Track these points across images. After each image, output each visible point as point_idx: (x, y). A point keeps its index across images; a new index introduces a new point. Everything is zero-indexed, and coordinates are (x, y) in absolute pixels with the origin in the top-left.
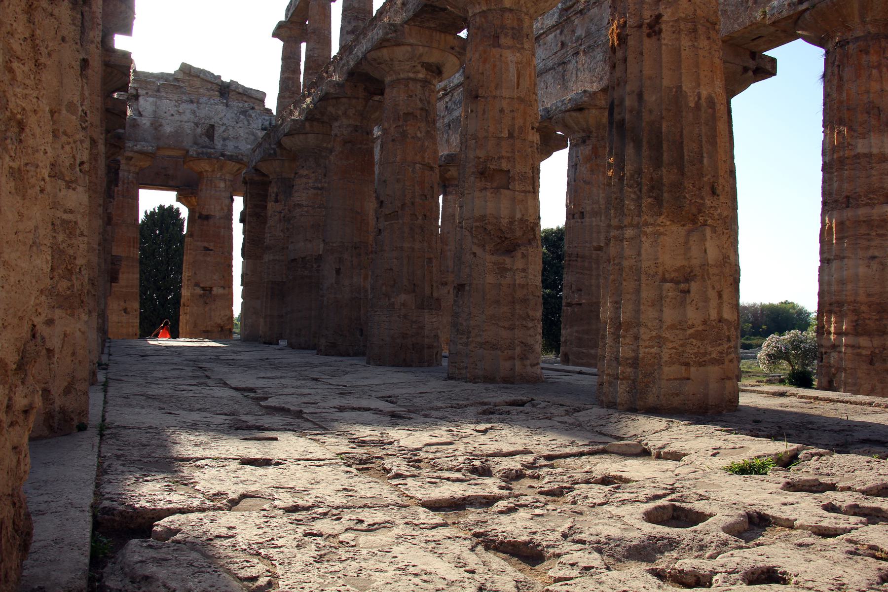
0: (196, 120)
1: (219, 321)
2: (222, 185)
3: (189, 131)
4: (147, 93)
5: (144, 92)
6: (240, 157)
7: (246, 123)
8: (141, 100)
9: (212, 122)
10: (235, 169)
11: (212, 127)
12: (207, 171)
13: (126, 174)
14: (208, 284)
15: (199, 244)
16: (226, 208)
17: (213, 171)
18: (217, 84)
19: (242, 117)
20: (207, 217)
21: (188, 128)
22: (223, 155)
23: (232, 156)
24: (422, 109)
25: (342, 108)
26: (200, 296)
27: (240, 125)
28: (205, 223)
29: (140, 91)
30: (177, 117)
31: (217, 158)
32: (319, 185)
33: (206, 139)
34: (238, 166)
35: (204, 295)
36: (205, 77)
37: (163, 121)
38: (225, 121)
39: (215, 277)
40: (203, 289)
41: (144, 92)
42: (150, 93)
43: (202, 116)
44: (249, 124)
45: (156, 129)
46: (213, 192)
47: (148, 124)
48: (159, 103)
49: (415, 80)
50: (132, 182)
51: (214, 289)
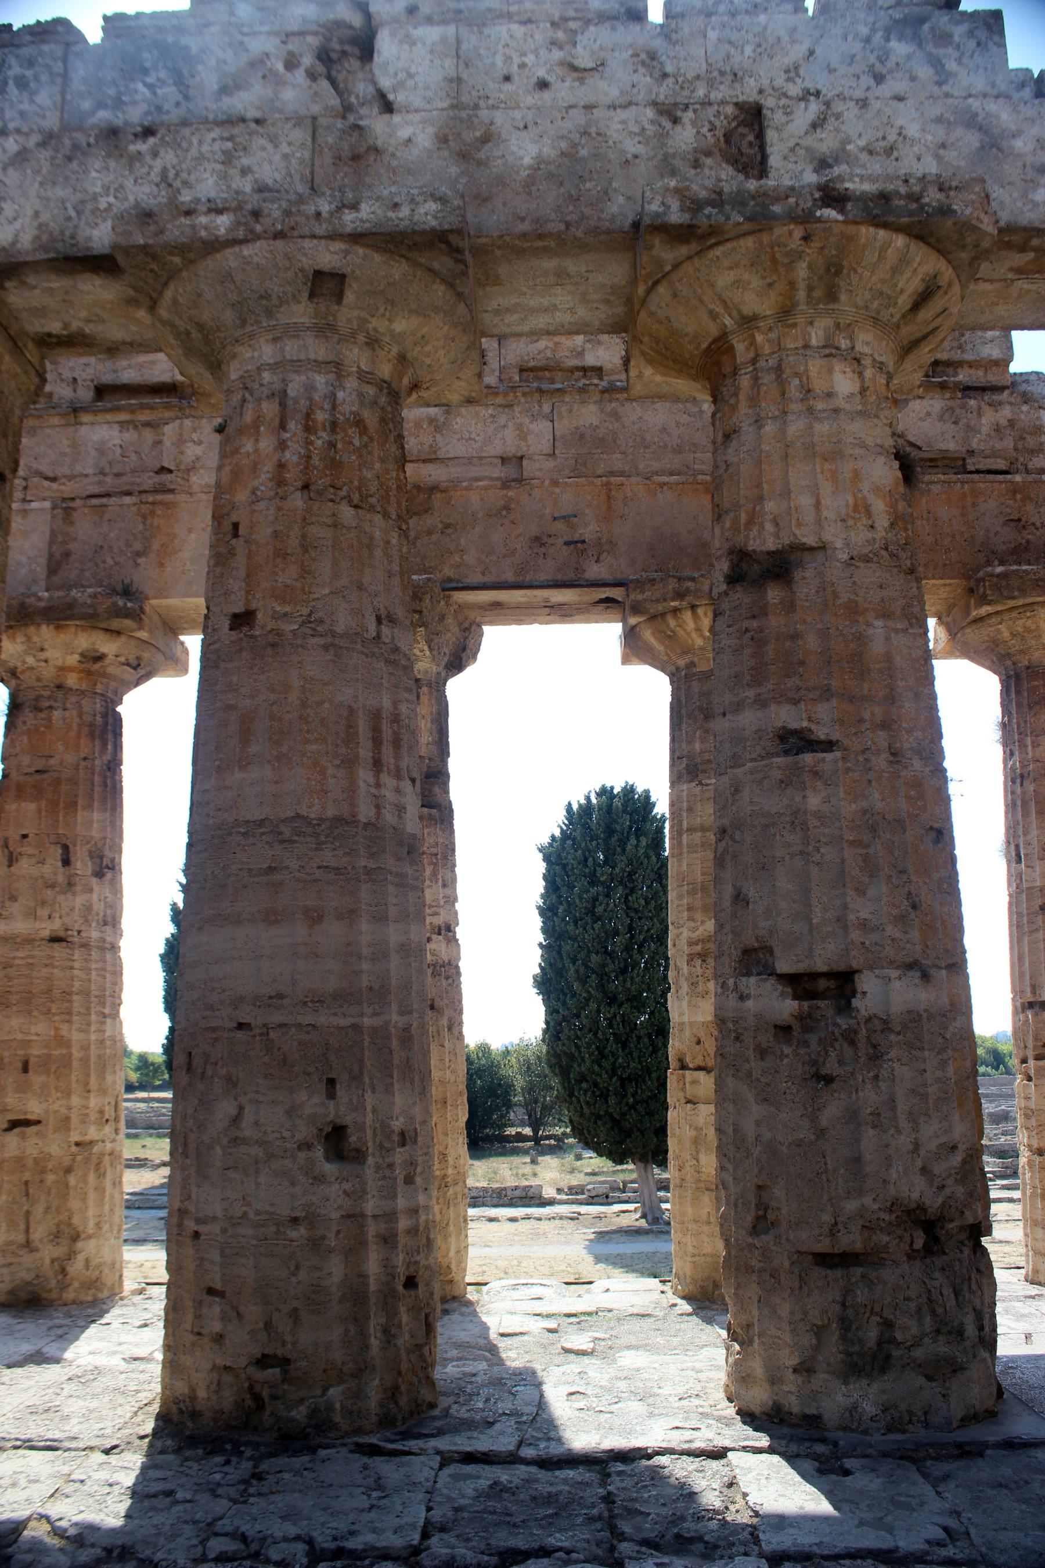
0: (664, 92)
1: (915, 1189)
2: (844, 383)
3: (632, 146)
6: (932, 197)
7: (925, 72)
8: (386, 45)
9: (748, 92)
10: (910, 285)
11: (753, 116)
12: (749, 322)
13: (321, 380)
14: (824, 957)
15: (749, 719)
17: (786, 312)
19: (899, 48)
20: (780, 567)
21: (627, 131)
22: (832, 196)
23: (884, 197)
26: (783, 1030)
27: (896, 85)
28: (774, 594)
30: (564, 91)
31: (806, 218)
33: (727, 172)
34: (926, 263)
35: (807, 1021)
37: (499, 117)
38: (814, 77)
39: (861, 909)
40: (800, 984)
43: (694, 67)
44: (942, 76)
45: (463, 156)
46: (795, 427)
47: (425, 139)
48: (470, 40)
50: (359, 423)
51: (867, 983)
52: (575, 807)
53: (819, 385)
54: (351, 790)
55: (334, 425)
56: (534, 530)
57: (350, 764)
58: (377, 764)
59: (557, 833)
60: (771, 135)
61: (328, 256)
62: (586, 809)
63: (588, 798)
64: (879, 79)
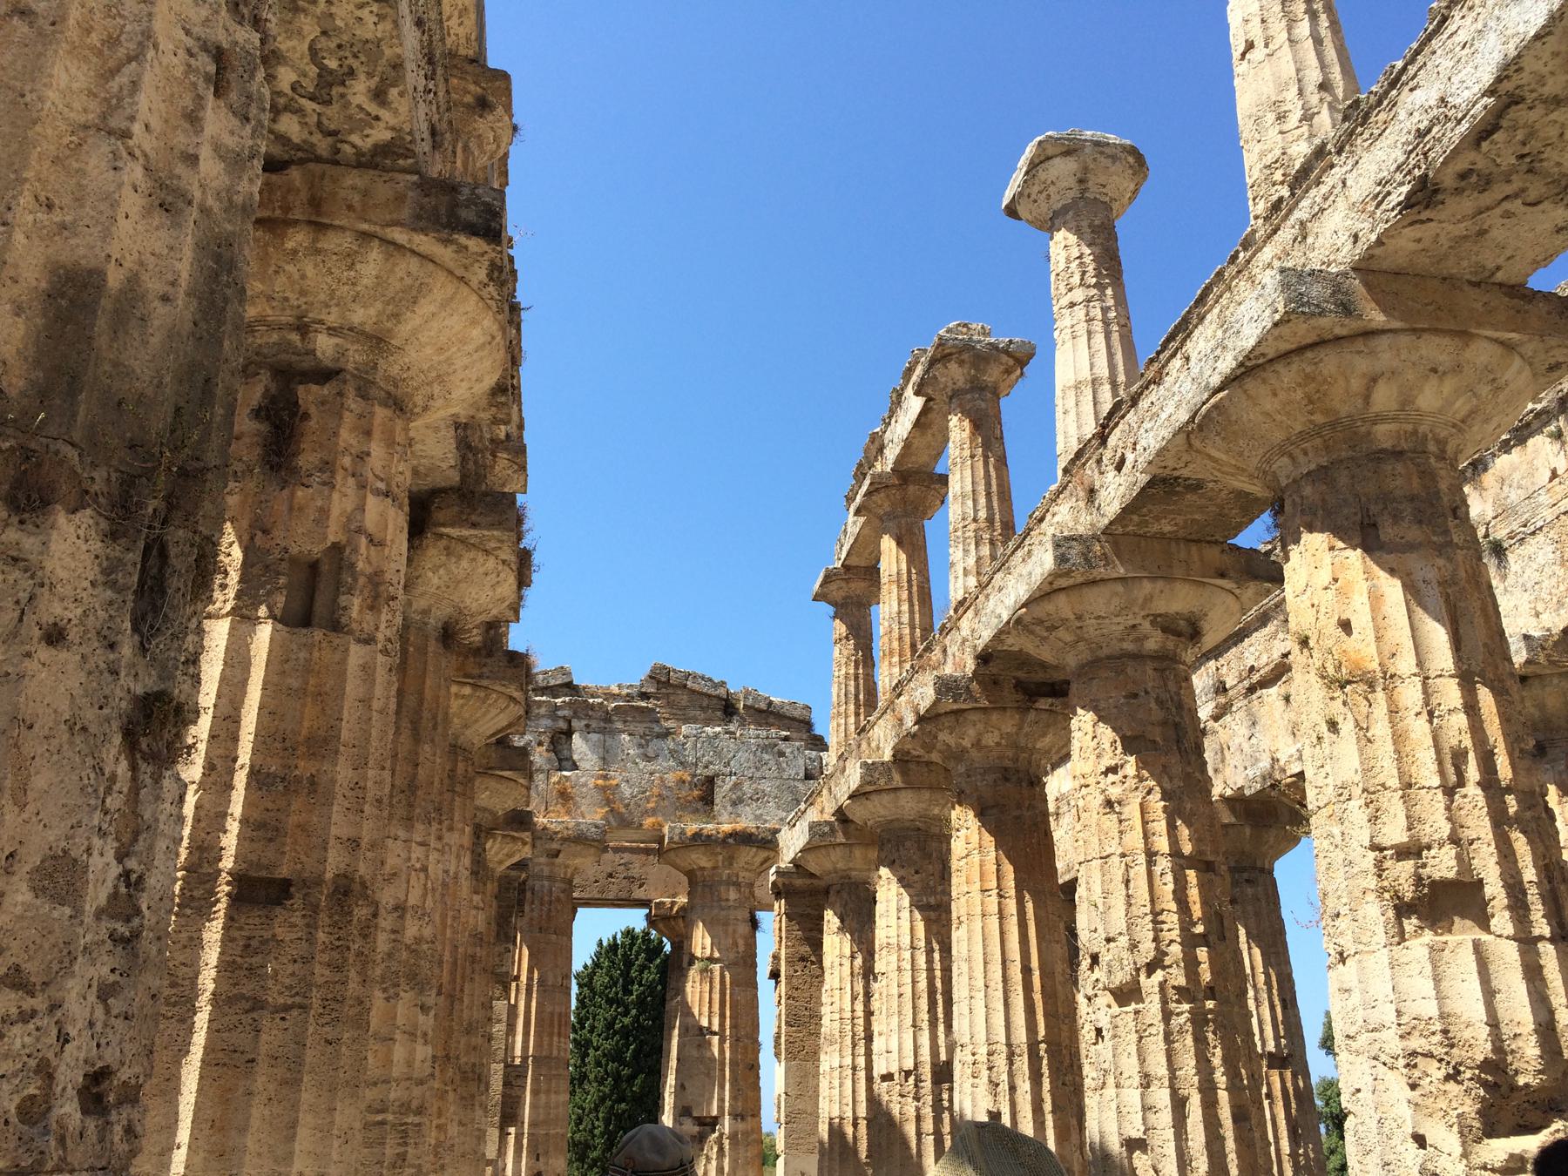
4: (587, 726)
5: (584, 722)
10: (758, 860)
16: (741, 942)
18: (718, 697)
19: (766, 757)
24: (1164, 723)
25: (972, 732)
27: (764, 771)
29: (575, 723)
32: (932, 900)
36: (696, 687)
41: (584, 722)
42: (594, 724)
48: (609, 741)
49: (1138, 657)
52: (605, 944)
53: (724, 896)
54: (551, 1045)
55: (550, 903)
56: (609, 870)
57: (551, 1035)
58: (559, 1035)
59: (589, 962)
60: (717, 790)
61: (555, 846)
62: (613, 947)
63: (615, 938)
64: (757, 769)
